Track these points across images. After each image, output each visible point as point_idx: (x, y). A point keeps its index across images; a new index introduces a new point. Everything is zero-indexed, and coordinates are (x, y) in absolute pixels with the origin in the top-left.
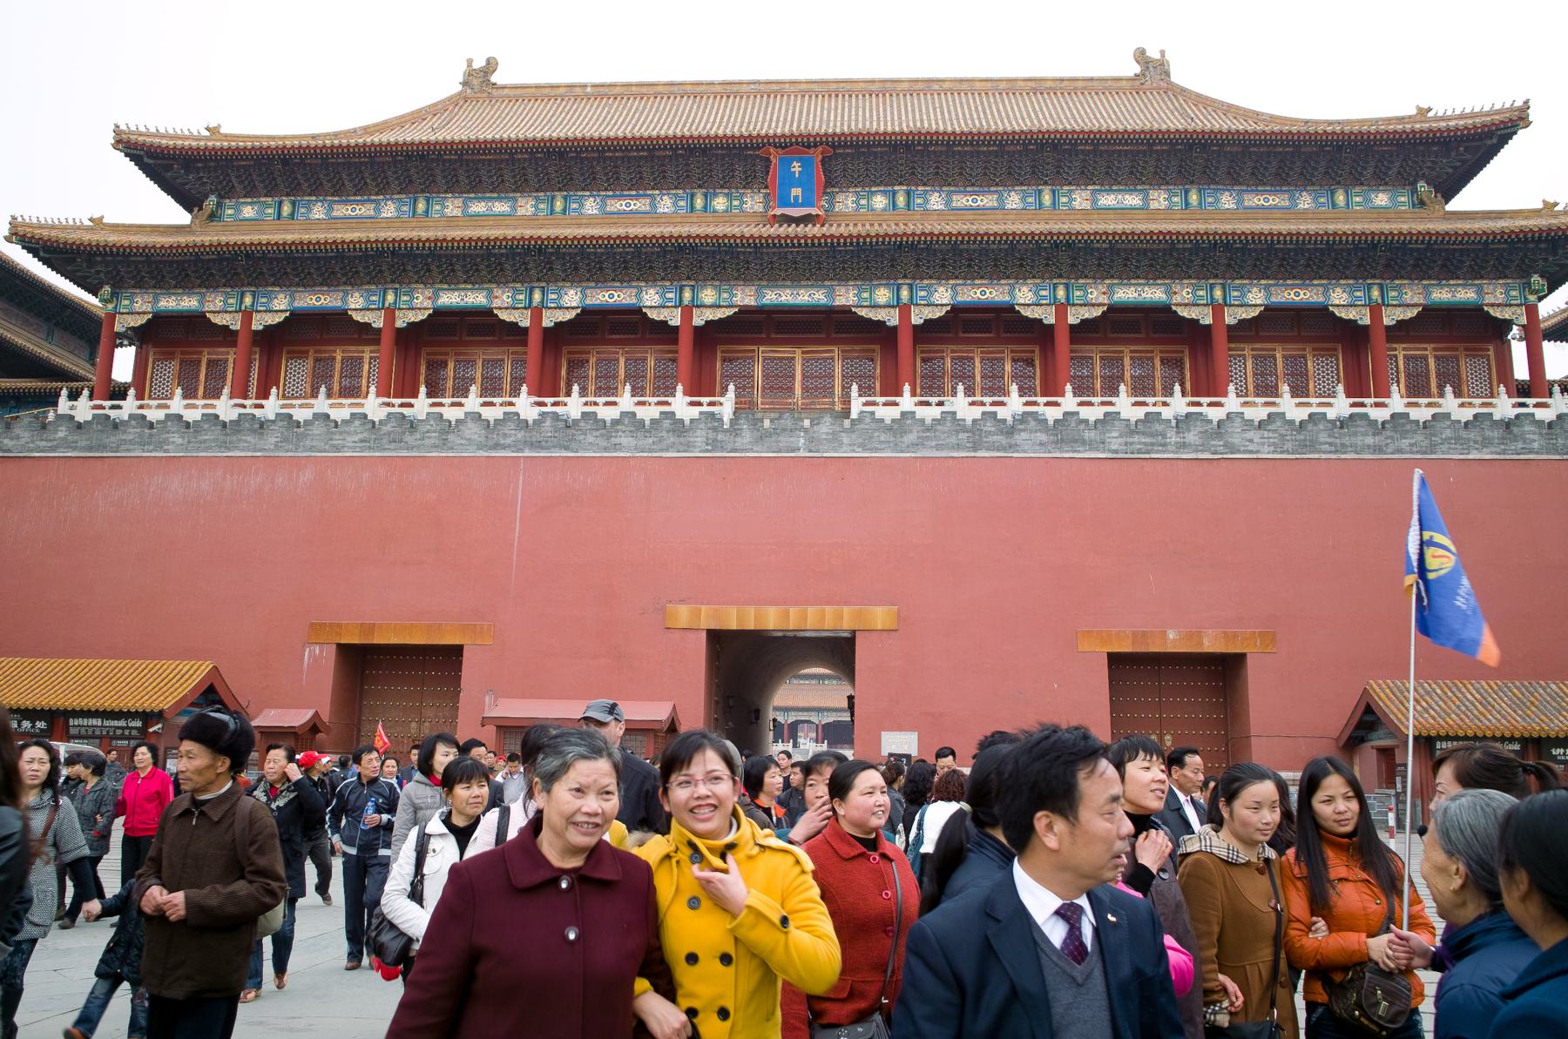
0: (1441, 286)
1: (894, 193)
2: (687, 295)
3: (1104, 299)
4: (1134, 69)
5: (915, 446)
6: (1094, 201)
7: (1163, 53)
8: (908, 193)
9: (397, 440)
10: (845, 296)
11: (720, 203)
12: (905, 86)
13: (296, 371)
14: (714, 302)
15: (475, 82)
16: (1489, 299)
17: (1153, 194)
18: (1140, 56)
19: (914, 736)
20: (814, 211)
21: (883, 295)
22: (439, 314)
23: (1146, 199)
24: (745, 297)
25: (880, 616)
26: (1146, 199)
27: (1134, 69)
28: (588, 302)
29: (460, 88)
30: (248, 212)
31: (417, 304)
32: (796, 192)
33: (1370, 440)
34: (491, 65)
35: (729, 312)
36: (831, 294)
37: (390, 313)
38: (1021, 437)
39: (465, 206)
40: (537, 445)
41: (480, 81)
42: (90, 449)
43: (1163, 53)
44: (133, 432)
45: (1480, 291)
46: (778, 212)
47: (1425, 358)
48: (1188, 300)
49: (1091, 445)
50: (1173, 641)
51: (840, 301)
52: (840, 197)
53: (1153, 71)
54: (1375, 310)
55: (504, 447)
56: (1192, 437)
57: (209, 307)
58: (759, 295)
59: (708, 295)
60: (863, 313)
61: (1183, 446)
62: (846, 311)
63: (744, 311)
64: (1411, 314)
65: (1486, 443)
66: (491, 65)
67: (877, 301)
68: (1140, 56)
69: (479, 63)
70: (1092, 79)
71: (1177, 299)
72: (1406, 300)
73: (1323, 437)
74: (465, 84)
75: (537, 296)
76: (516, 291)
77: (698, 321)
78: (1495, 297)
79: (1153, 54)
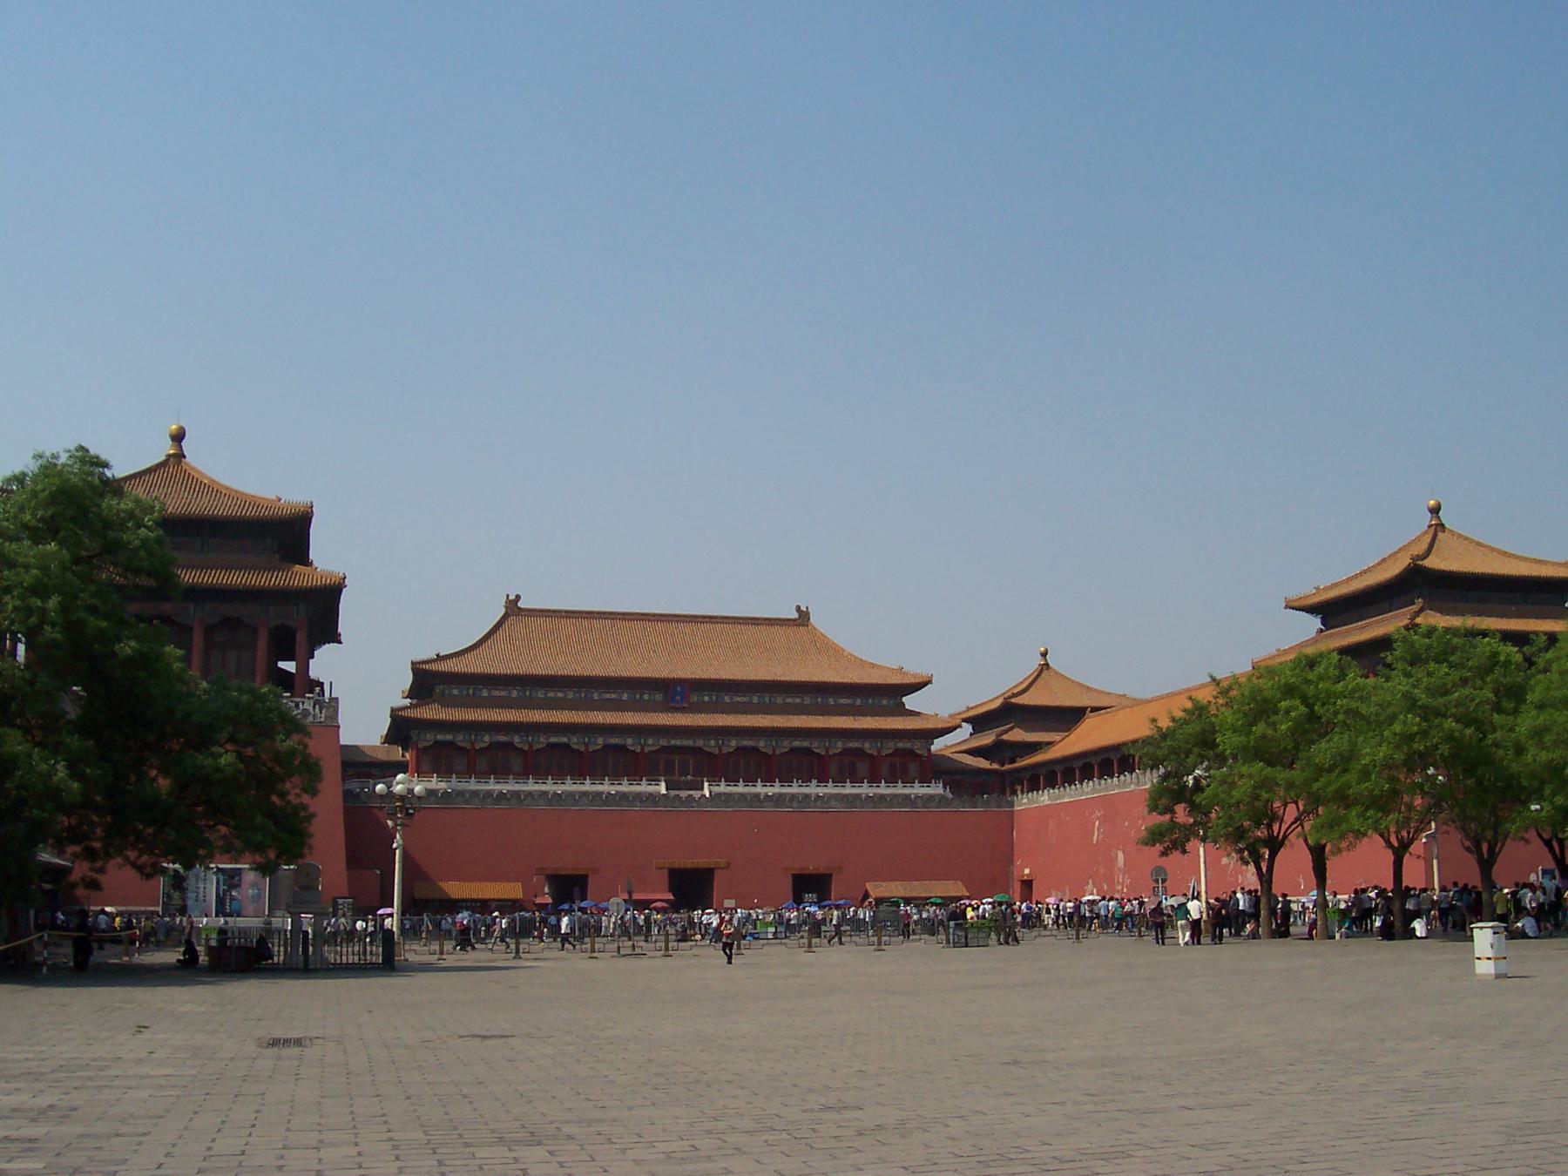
4: (795, 615)
10: (700, 743)
11: (646, 697)
14: (652, 744)
18: (798, 608)
21: (713, 743)
24: (663, 742)
25: (722, 862)
27: (795, 615)
29: (503, 611)
30: (455, 692)
31: (542, 741)
34: (518, 597)
53: (803, 617)
59: (650, 741)
66: (518, 597)
67: (711, 745)
68: (798, 608)
69: (512, 597)
78: (917, 747)
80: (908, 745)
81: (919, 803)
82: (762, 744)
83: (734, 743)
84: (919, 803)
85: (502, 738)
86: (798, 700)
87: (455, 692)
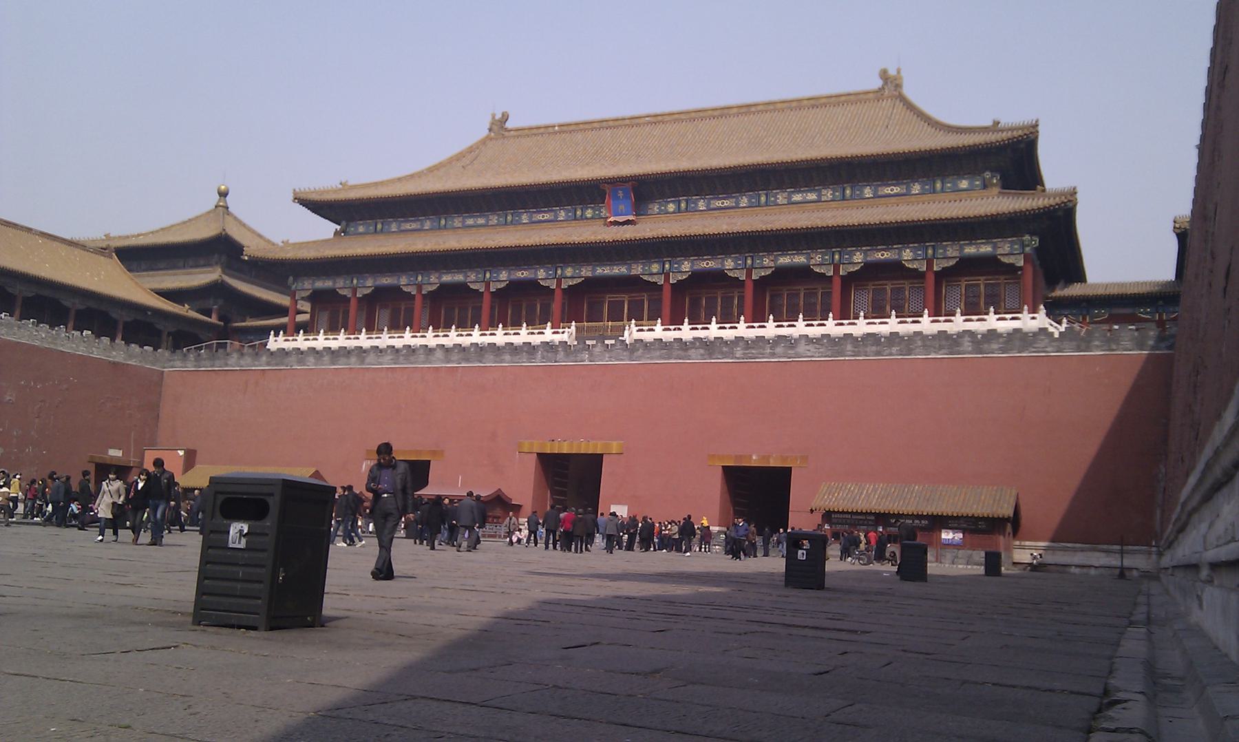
0: (970, 244)
1: (679, 202)
2: (559, 272)
3: (772, 264)
4: (879, 83)
5: (639, 358)
6: (789, 198)
7: (899, 71)
8: (687, 201)
9: (407, 357)
10: (637, 269)
11: (589, 213)
12: (735, 110)
13: (383, 315)
14: (572, 275)
15: (495, 128)
16: (1000, 251)
17: (824, 192)
18: (884, 75)
19: (626, 508)
20: (631, 218)
21: (655, 268)
22: (444, 287)
23: (819, 196)
24: (586, 272)
25: (615, 447)
26: (819, 196)
27: (879, 83)
28: (513, 277)
32: (622, 207)
33: (874, 348)
34: (505, 117)
35: (580, 280)
36: (629, 269)
37: (420, 287)
38: (692, 352)
39: (463, 222)
40: (467, 360)
41: (499, 125)
42: (277, 365)
43: (899, 71)
44: (293, 358)
45: (995, 247)
46: (612, 219)
47: (978, 285)
48: (818, 261)
49: (725, 355)
50: (755, 460)
51: (634, 272)
52: (651, 206)
54: (930, 264)
55: (453, 362)
56: (779, 350)
57: (338, 285)
58: (594, 270)
59: (569, 271)
60: (645, 278)
61: (773, 355)
62: (637, 278)
63: (587, 279)
64: (952, 263)
65: (941, 347)
66: (505, 117)
68: (884, 75)
69: (499, 116)
70: (849, 95)
71: (813, 262)
72: (950, 254)
73: (849, 347)
74: (490, 130)
75: (488, 275)
76: (478, 273)
77: (564, 286)
79: (892, 72)
80: (986, 249)
81: (967, 344)
82: (729, 264)
83: (686, 266)
84: (967, 344)
85: (386, 281)
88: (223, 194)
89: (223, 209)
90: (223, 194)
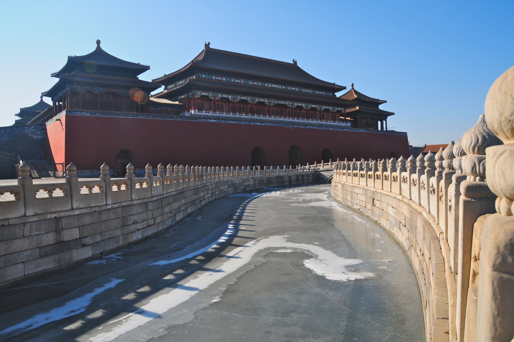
4: (293, 63)
10: (287, 103)
18: (293, 60)
21: (290, 103)
24: (276, 102)
27: (293, 63)
30: (204, 76)
34: (209, 43)
41: (207, 46)
53: (295, 63)
59: (272, 102)
63: (276, 105)
66: (209, 43)
68: (293, 60)
69: (207, 43)
86: (308, 91)
87: (204, 76)
88: (98, 42)
89: (99, 48)
90: (98, 42)
